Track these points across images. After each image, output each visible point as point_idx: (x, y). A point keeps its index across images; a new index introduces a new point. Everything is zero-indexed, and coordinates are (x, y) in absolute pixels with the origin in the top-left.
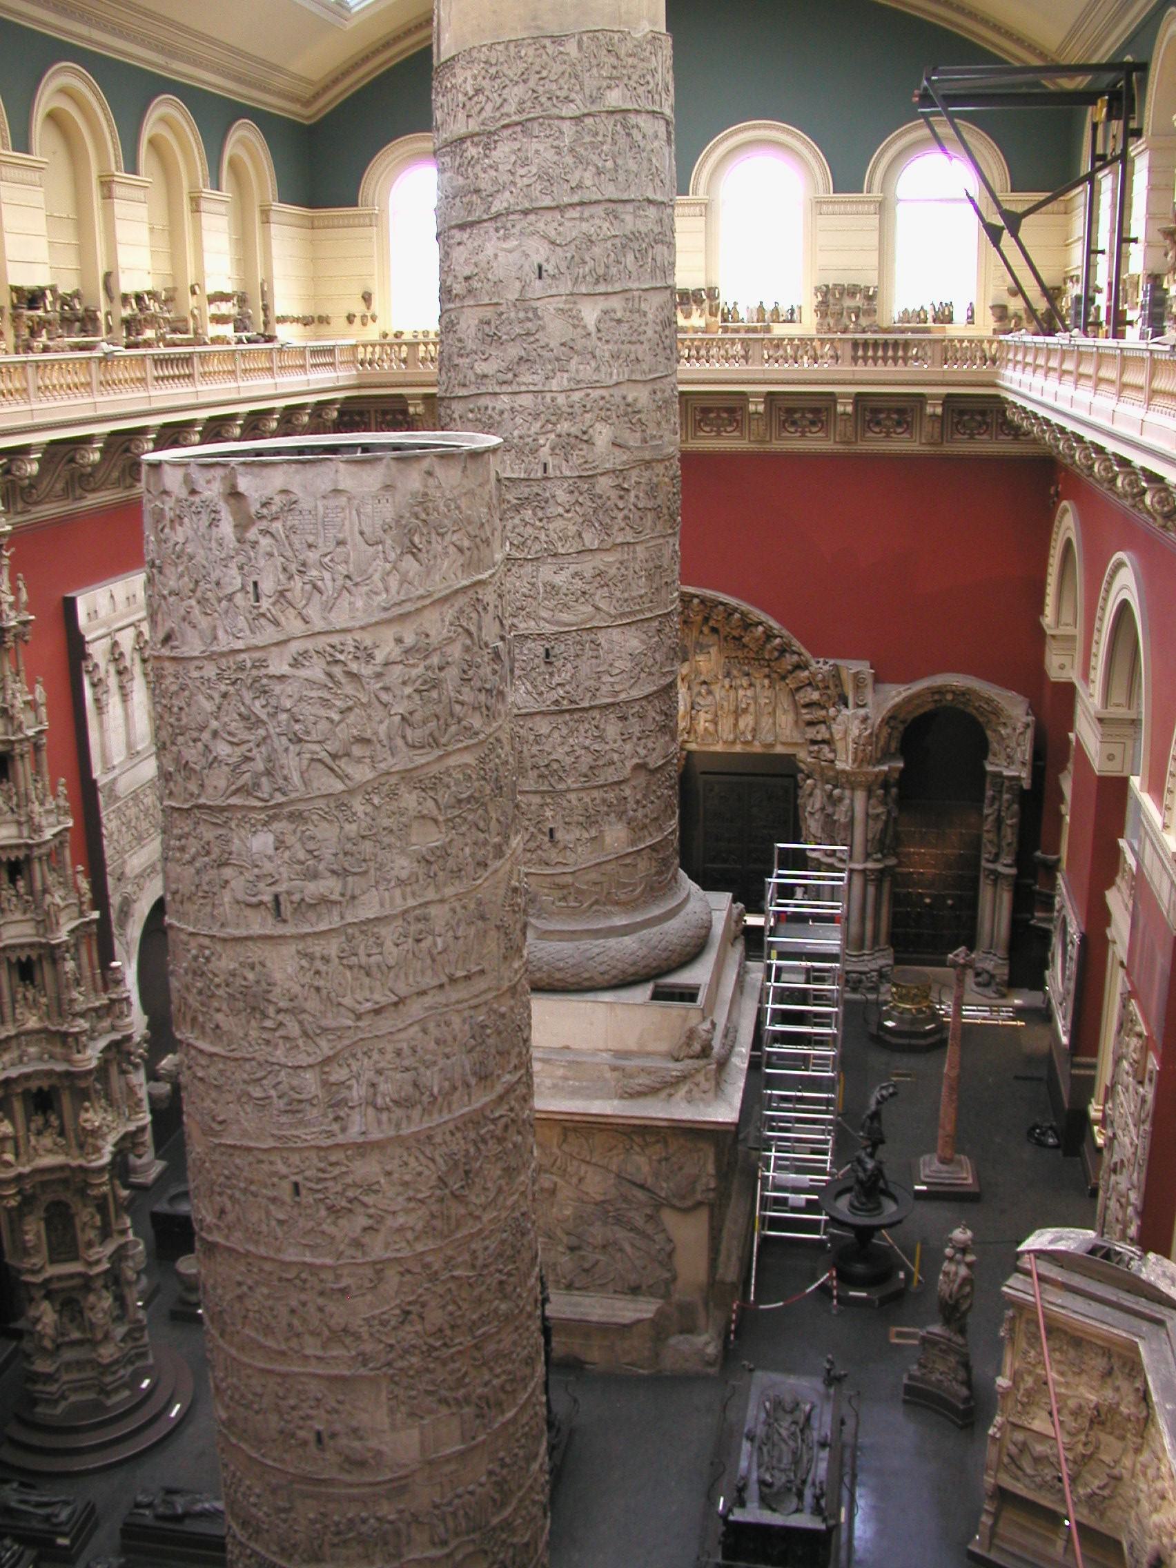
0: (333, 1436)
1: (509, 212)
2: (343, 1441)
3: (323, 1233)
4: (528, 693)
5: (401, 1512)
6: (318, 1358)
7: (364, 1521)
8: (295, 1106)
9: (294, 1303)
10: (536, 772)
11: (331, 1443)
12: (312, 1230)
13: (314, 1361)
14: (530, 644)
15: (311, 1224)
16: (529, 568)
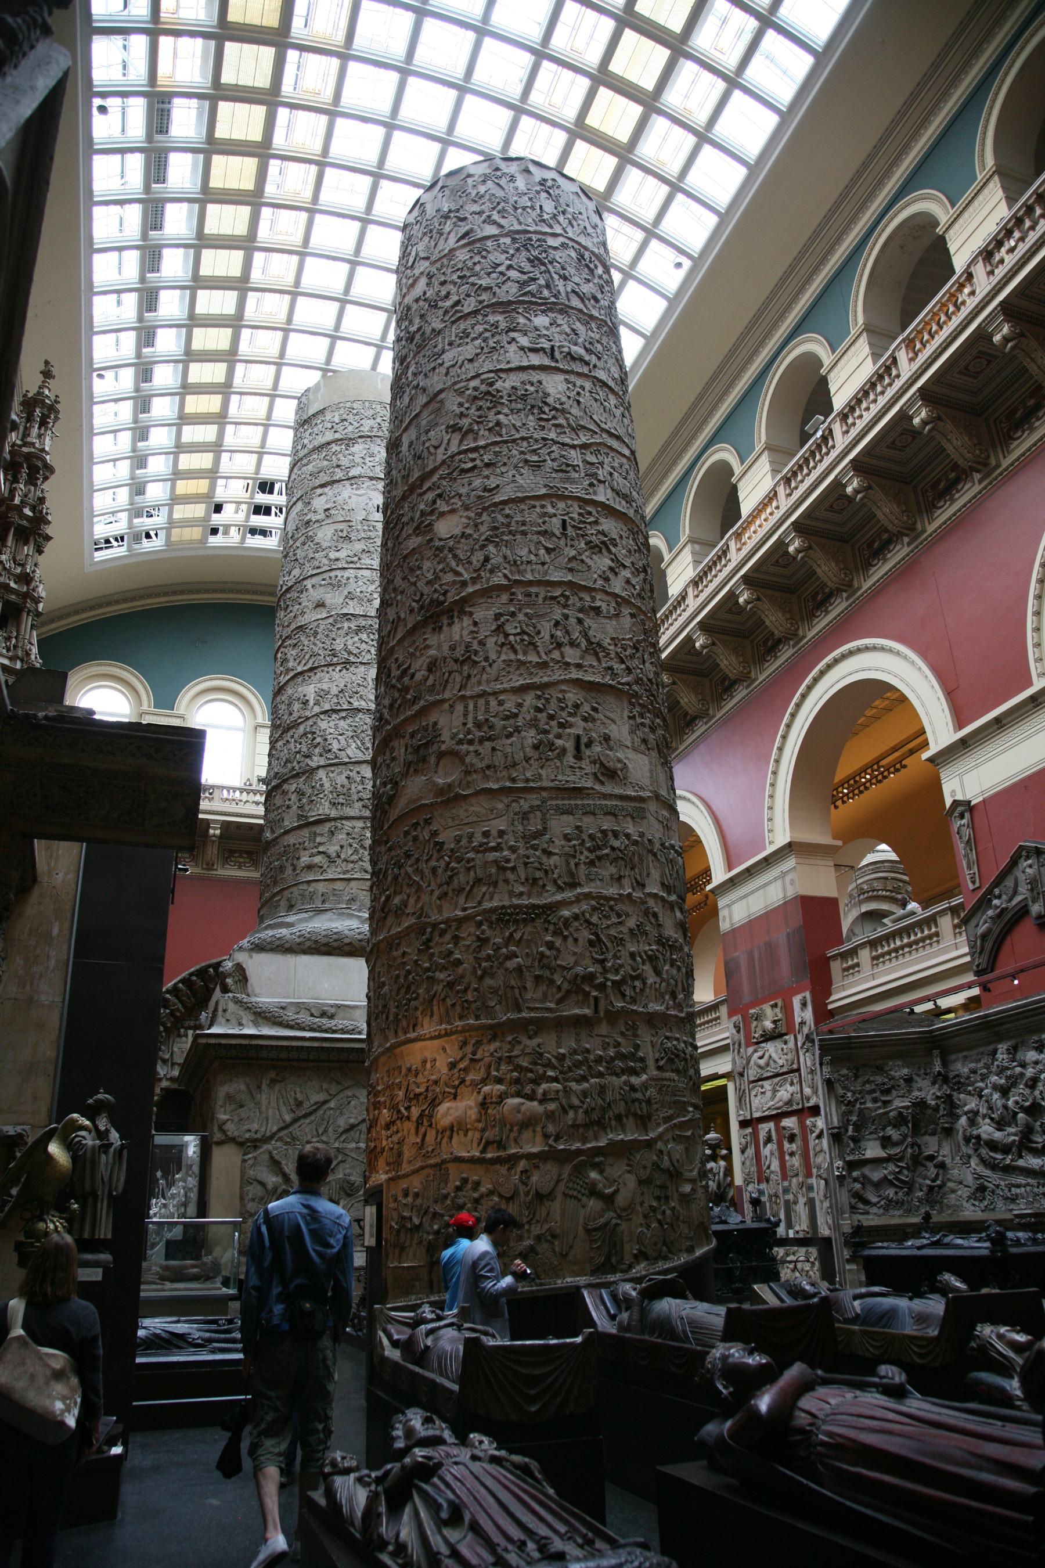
0: (588, 745)
1: (360, 476)
2: (597, 749)
3: (582, 561)
4: (358, 748)
5: (642, 835)
6: (579, 666)
7: (616, 835)
8: (564, 467)
9: (558, 617)
10: (360, 804)
11: (588, 752)
12: (574, 558)
13: (573, 669)
14: (360, 715)
15: (573, 553)
16: (362, 668)
